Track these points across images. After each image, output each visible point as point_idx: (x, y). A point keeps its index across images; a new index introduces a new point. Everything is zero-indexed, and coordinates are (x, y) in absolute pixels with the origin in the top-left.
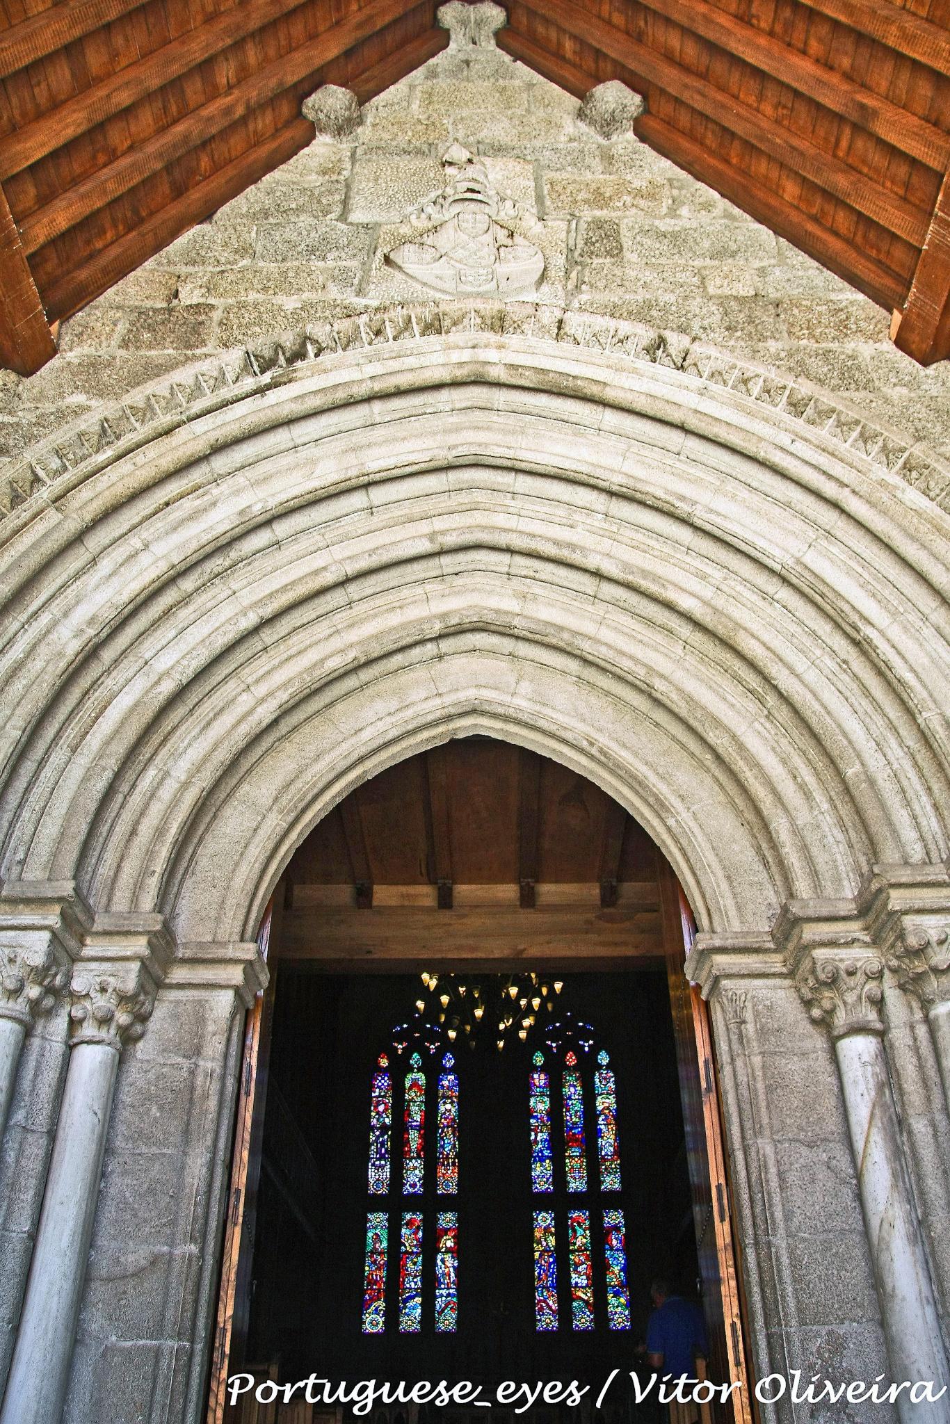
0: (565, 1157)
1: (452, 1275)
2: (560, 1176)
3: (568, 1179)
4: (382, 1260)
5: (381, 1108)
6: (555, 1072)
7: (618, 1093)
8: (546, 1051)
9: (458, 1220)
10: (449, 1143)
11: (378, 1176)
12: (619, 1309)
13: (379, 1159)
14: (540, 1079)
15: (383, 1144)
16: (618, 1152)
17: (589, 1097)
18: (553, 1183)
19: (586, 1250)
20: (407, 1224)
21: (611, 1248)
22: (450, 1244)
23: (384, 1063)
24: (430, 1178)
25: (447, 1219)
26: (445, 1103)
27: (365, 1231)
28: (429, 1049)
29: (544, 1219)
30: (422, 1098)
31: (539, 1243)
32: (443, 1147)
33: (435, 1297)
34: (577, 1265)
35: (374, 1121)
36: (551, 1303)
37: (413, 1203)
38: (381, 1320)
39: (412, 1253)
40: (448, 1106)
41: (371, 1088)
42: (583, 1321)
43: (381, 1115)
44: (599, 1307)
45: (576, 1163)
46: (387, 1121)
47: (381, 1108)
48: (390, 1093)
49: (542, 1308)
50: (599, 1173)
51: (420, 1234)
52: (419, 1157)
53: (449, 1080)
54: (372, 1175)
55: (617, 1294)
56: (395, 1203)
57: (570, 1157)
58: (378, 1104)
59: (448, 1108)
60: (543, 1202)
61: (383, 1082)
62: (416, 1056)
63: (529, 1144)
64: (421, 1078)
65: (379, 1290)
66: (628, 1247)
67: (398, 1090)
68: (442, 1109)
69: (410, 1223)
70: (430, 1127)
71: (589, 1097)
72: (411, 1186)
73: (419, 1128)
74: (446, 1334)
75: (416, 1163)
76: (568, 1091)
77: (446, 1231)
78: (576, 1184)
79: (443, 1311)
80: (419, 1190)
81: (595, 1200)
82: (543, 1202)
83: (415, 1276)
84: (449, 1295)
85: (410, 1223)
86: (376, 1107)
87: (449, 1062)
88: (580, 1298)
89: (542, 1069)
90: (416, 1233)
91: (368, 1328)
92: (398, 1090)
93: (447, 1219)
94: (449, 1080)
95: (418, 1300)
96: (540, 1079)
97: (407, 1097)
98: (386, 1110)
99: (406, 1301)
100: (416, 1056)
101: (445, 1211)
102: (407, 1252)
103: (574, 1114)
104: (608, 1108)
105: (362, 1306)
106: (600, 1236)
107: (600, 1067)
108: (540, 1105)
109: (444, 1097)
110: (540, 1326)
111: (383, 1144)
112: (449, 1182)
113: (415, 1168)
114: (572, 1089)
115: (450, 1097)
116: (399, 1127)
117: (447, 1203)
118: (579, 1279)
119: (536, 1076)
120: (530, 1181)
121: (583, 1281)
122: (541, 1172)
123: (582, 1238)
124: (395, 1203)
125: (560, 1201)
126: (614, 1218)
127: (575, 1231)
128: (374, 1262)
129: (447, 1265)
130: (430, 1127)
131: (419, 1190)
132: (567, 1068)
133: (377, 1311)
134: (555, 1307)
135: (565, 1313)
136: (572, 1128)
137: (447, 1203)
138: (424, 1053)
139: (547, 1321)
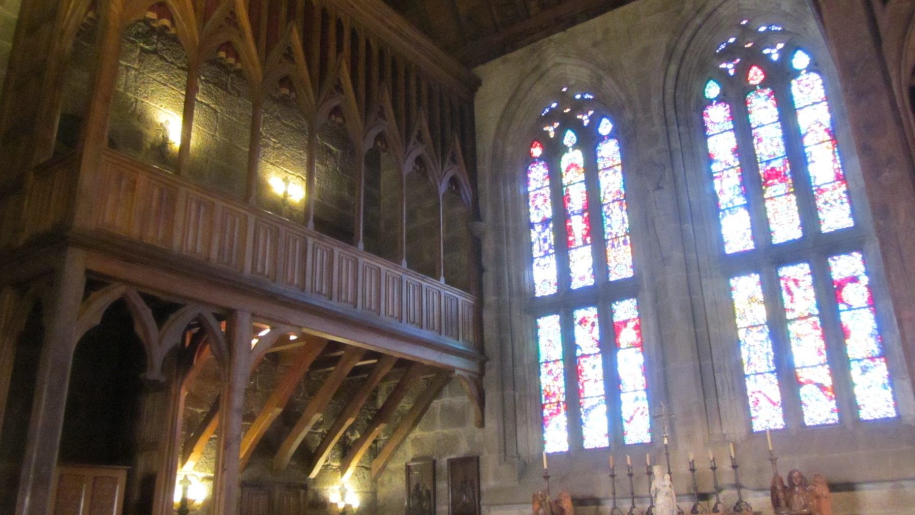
0: (764, 200)
1: (639, 372)
2: (761, 226)
3: (772, 227)
4: (559, 368)
5: (539, 201)
6: (736, 96)
8: (722, 77)
10: (617, 221)
13: (544, 257)
19: (810, 315)
20: (580, 323)
21: (850, 308)
23: (537, 151)
25: (625, 310)
27: (536, 338)
28: (581, 121)
29: (746, 290)
30: (582, 177)
31: (744, 316)
32: (609, 226)
35: (535, 218)
37: (586, 298)
39: (588, 356)
43: (540, 208)
44: (842, 389)
48: (547, 182)
49: (757, 403)
52: (585, 243)
55: (864, 370)
56: (565, 302)
57: (771, 198)
58: (535, 196)
59: (612, 182)
61: (538, 174)
65: (558, 402)
67: (555, 176)
69: (583, 321)
76: (755, 118)
77: (625, 323)
79: (632, 418)
80: (590, 281)
81: (816, 248)
83: (596, 381)
84: (637, 399)
85: (583, 321)
86: (533, 201)
87: (605, 127)
88: (811, 382)
89: (720, 99)
90: (591, 332)
92: (555, 176)
94: (609, 151)
95: (603, 408)
97: (565, 181)
98: (545, 201)
101: (621, 299)
102: (583, 356)
103: (769, 144)
105: (541, 422)
106: (829, 294)
107: (796, 74)
111: (545, 240)
112: (621, 264)
115: (610, 168)
117: (623, 290)
120: (721, 243)
124: (565, 302)
126: (845, 265)
127: (790, 293)
128: (550, 372)
129: (631, 363)
132: (753, 88)
134: (777, 396)
135: (791, 403)
136: (768, 162)
137: (623, 290)
138: (578, 127)
139: (767, 416)
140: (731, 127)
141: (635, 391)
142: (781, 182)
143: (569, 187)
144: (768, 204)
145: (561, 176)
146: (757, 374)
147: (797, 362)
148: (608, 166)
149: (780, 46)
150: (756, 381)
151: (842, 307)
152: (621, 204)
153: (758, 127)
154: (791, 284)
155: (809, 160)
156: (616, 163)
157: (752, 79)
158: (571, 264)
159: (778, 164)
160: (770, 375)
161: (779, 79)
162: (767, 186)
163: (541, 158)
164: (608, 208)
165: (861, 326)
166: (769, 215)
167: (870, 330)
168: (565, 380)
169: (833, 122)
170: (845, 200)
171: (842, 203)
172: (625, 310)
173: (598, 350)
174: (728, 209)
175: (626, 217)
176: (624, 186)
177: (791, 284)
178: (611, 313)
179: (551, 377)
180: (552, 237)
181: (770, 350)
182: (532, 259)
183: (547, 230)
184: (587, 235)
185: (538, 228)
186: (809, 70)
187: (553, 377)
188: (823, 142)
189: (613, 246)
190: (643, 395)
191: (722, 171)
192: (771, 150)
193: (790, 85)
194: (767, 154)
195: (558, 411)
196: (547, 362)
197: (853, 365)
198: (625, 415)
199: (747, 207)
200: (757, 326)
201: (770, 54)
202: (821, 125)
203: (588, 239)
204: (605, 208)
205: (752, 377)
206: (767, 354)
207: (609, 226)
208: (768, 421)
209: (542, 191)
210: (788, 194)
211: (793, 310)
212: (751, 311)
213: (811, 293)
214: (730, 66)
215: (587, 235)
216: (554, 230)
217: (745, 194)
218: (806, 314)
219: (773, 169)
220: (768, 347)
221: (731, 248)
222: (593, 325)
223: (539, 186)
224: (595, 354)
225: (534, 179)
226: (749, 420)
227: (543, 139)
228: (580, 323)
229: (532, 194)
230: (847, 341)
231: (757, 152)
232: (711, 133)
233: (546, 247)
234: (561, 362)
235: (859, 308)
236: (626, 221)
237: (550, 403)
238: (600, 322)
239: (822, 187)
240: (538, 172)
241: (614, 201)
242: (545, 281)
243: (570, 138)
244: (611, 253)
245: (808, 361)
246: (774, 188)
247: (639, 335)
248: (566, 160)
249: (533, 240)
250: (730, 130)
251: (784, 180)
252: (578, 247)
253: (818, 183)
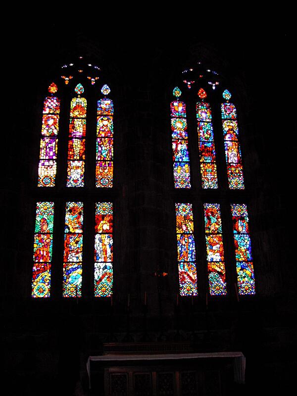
1: (109, 250)
2: (196, 176)
5: (51, 122)
7: (239, 119)
8: (183, 88)
9: (114, 209)
10: (105, 150)
11: (47, 172)
12: (246, 279)
13: (49, 160)
14: (179, 107)
15: (51, 149)
16: (241, 162)
17: (217, 122)
18: (191, 182)
19: (218, 233)
21: (239, 233)
22: (106, 227)
23: (53, 89)
24: (90, 174)
26: (102, 120)
27: (35, 215)
28: (90, 81)
29: (184, 210)
31: (180, 227)
32: (100, 152)
33: (93, 269)
34: (212, 245)
35: (44, 132)
36: (191, 274)
37: (75, 194)
38: (47, 287)
39: (74, 234)
40: (105, 123)
41: (43, 108)
42: (218, 286)
43: (50, 126)
44: (231, 276)
45: (209, 168)
46: (56, 132)
47: (51, 122)
48: (58, 112)
49: (184, 278)
50: (227, 176)
51: (82, 219)
52: (81, 159)
53: (106, 104)
54: (42, 172)
56: (60, 194)
58: (48, 118)
59: (104, 125)
60: (183, 196)
61: (52, 104)
62: (80, 86)
63: (172, 153)
64: (83, 102)
66: (252, 231)
68: (100, 124)
69: (72, 211)
70: (90, 137)
71: (217, 122)
72: (73, 180)
73: (81, 138)
74: (103, 299)
75: (80, 164)
77: (103, 217)
78: (210, 182)
79: (101, 280)
80: (80, 184)
81: (225, 197)
82: (183, 196)
83: (77, 252)
84: (106, 267)
86: (46, 121)
87: (106, 90)
89: (181, 99)
90: (78, 218)
91: (36, 294)
93: (104, 208)
94: (106, 104)
95: (80, 271)
96: (179, 107)
97: (72, 115)
98: (55, 123)
99: (69, 272)
100: (80, 86)
102: (70, 233)
104: (232, 130)
105: (30, 276)
107: (224, 101)
108: (179, 125)
109: (101, 115)
110: (183, 292)
112: (105, 177)
113: (78, 167)
114: (204, 115)
116: (64, 137)
117: (104, 195)
118: (214, 255)
119: (176, 104)
120: (172, 180)
121: (217, 257)
122: (182, 174)
123: (215, 224)
125: (196, 195)
126: (239, 210)
127: (209, 219)
128: (41, 241)
129: (103, 244)
130: (90, 137)
131: (80, 184)
132: (200, 100)
133: (44, 281)
134: (195, 277)
137: (104, 195)
138: (86, 84)
139: (188, 288)
140: (185, 116)
141: (105, 262)
142: (209, 156)
143: (76, 120)
144: (202, 166)
145: (70, 112)
146: (185, 262)
147: (209, 258)
148: (105, 114)
149: (217, 83)
150: (184, 266)
151: (235, 232)
152: (110, 140)
153: (201, 121)
154: (210, 214)
155: (226, 148)
156: (110, 114)
157: (200, 94)
158: (69, 170)
159: (209, 145)
160: (192, 264)
161: (215, 103)
162: (202, 156)
163: (55, 95)
164: (101, 140)
165: (244, 243)
166: (202, 172)
167: (248, 246)
168: (53, 248)
169: (239, 131)
170: (241, 175)
171: (240, 176)
172: (104, 208)
173: (80, 231)
174: (179, 161)
175: (112, 149)
176: (114, 129)
177: (210, 214)
178: (94, 209)
179: (41, 245)
180: (57, 148)
181: (194, 249)
182: (39, 160)
183: (54, 143)
184: (83, 154)
185: (47, 140)
186: (230, 101)
187: (43, 244)
188: (235, 141)
189: (101, 166)
190: (109, 265)
191: (178, 139)
192: (206, 135)
193: (221, 106)
194: (204, 137)
195: (44, 270)
196: (40, 234)
197: (237, 264)
198: (96, 278)
199: (190, 163)
200: (187, 234)
201: (212, 86)
202: (234, 132)
203: (84, 156)
204: (99, 140)
205: (182, 263)
206: (192, 251)
207: (100, 152)
208: (188, 290)
209: (55, 117)
210: (212, 163)
211: (210, 229)
212: (186, 225)
213: (220, 220)
214: (189, 83)
215: (83, 154)
216: (58, 144)
217: (190, 156)
218: (216, 232)
219: (206, 147)
220: (192, 248)
221: (179, 185)
222: (80, 214)
223: (51, 112)
224: (78, 233)
225: (49, 107)
226: (178, 289)
227: (60, 84)
228: (70, 211)
229: (45, 117)
230: (236, 250)
231: (199, 135)
232: (174, 116)
233: (51, 154)
234: (52, 235)
235: (244, 234)
236: (112, 151)
237: (39, 262)
238: (84, 213)
239: (232, 164)
240: (52, 103)
241: (105, 137)
242: (47, 176)
243: (79, 88)
244: (99, 171)
245: (215, 258)
246: (206, 158)
247: (110, 226)
248: (74, 103)
249: (41, 146)
250: (184, 118)
251: (211, 155)
252: (75, 160)
253: (230, 161)
